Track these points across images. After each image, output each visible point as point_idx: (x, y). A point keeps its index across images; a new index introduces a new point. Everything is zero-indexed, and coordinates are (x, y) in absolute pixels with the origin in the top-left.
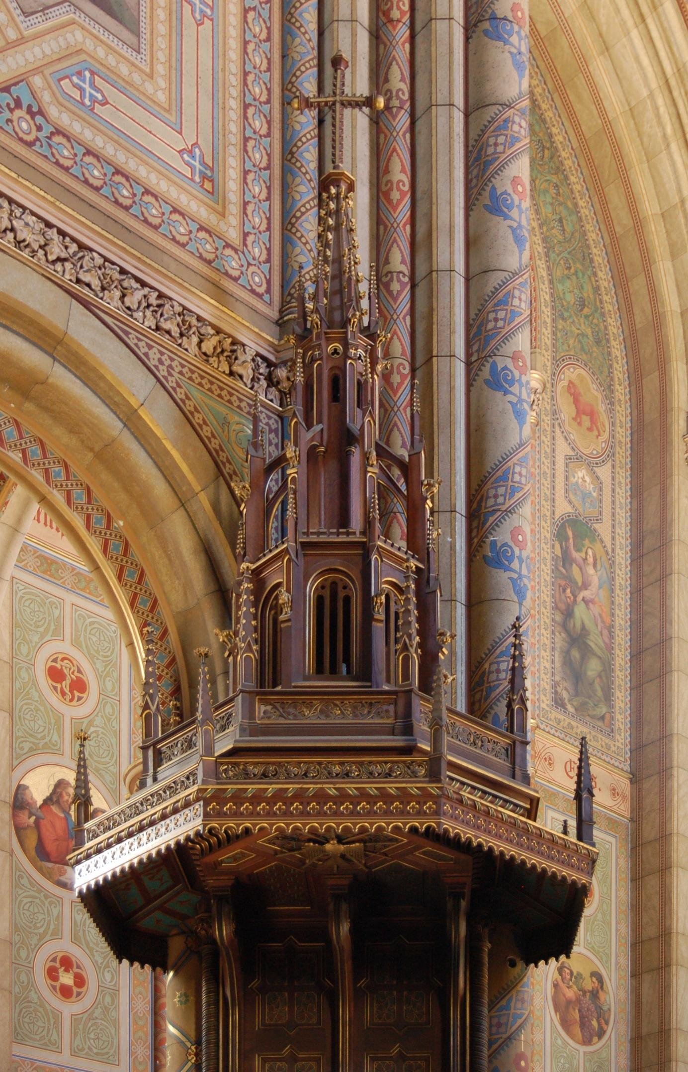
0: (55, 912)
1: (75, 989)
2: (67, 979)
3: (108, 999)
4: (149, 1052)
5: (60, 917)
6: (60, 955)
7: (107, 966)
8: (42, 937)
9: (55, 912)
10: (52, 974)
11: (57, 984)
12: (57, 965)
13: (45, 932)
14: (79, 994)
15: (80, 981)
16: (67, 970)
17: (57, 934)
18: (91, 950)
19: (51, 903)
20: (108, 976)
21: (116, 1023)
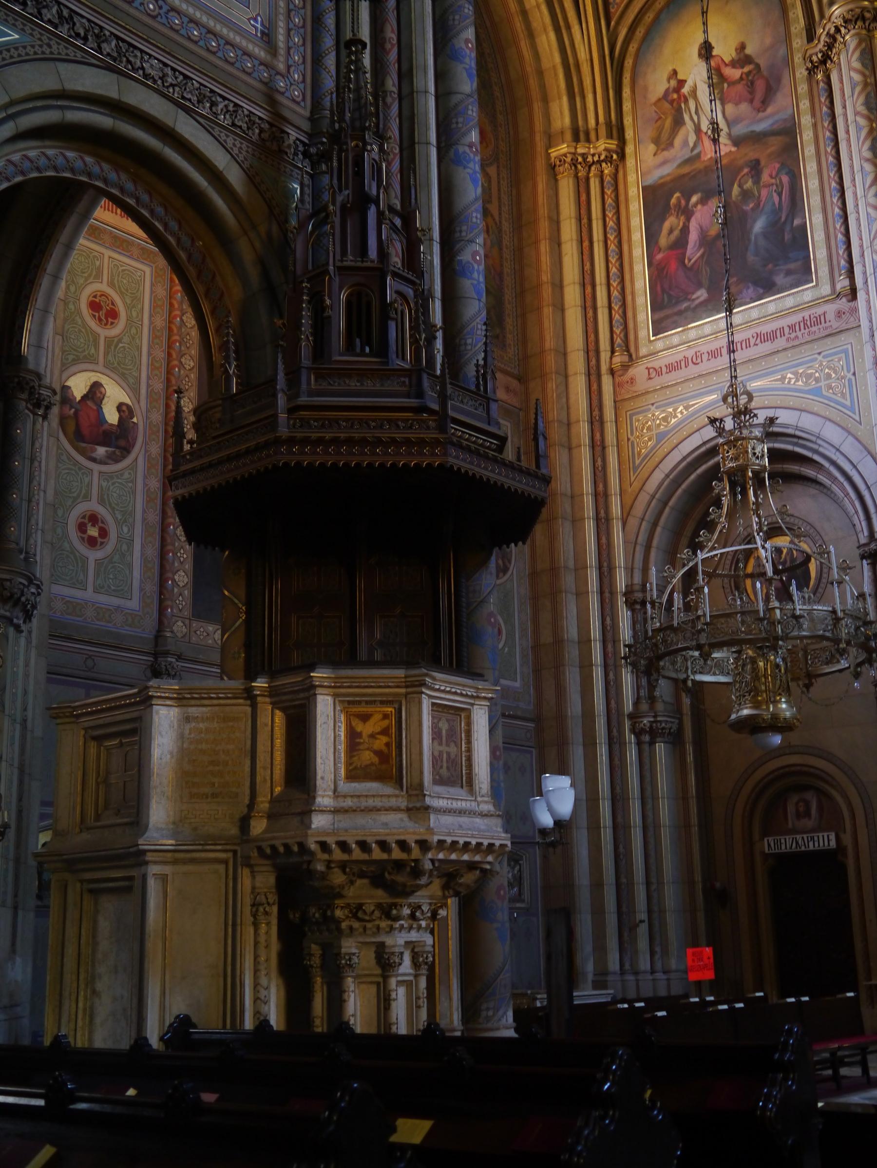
0: (87, 480)
1: (99, 540)
2: (93, 532)
3: (125, 547)
4: (156, 588)
5: (90, 485)
6: (88, 514)
7: (125, 521)
8: (75, 499)
9: (87, 480)
10: (82, 528)
11: (85, 536)
12: (86, 521)
13: (78, 496)
14: (102, 543)
15: (104, 533)
16: (93, 525)
17: (87, 497)
18: (113, 509)
19: (83, 474)
20: (125, 529)
21: (130, 566)
